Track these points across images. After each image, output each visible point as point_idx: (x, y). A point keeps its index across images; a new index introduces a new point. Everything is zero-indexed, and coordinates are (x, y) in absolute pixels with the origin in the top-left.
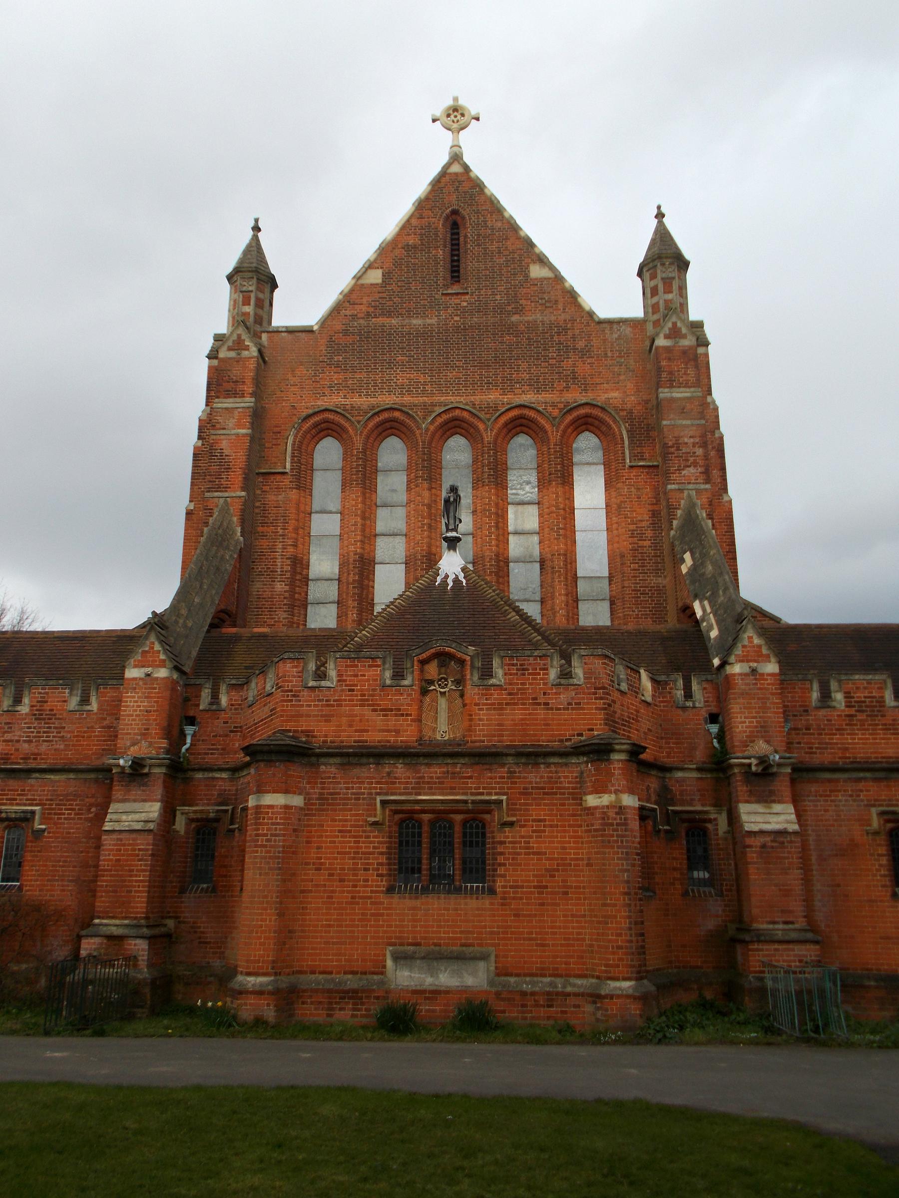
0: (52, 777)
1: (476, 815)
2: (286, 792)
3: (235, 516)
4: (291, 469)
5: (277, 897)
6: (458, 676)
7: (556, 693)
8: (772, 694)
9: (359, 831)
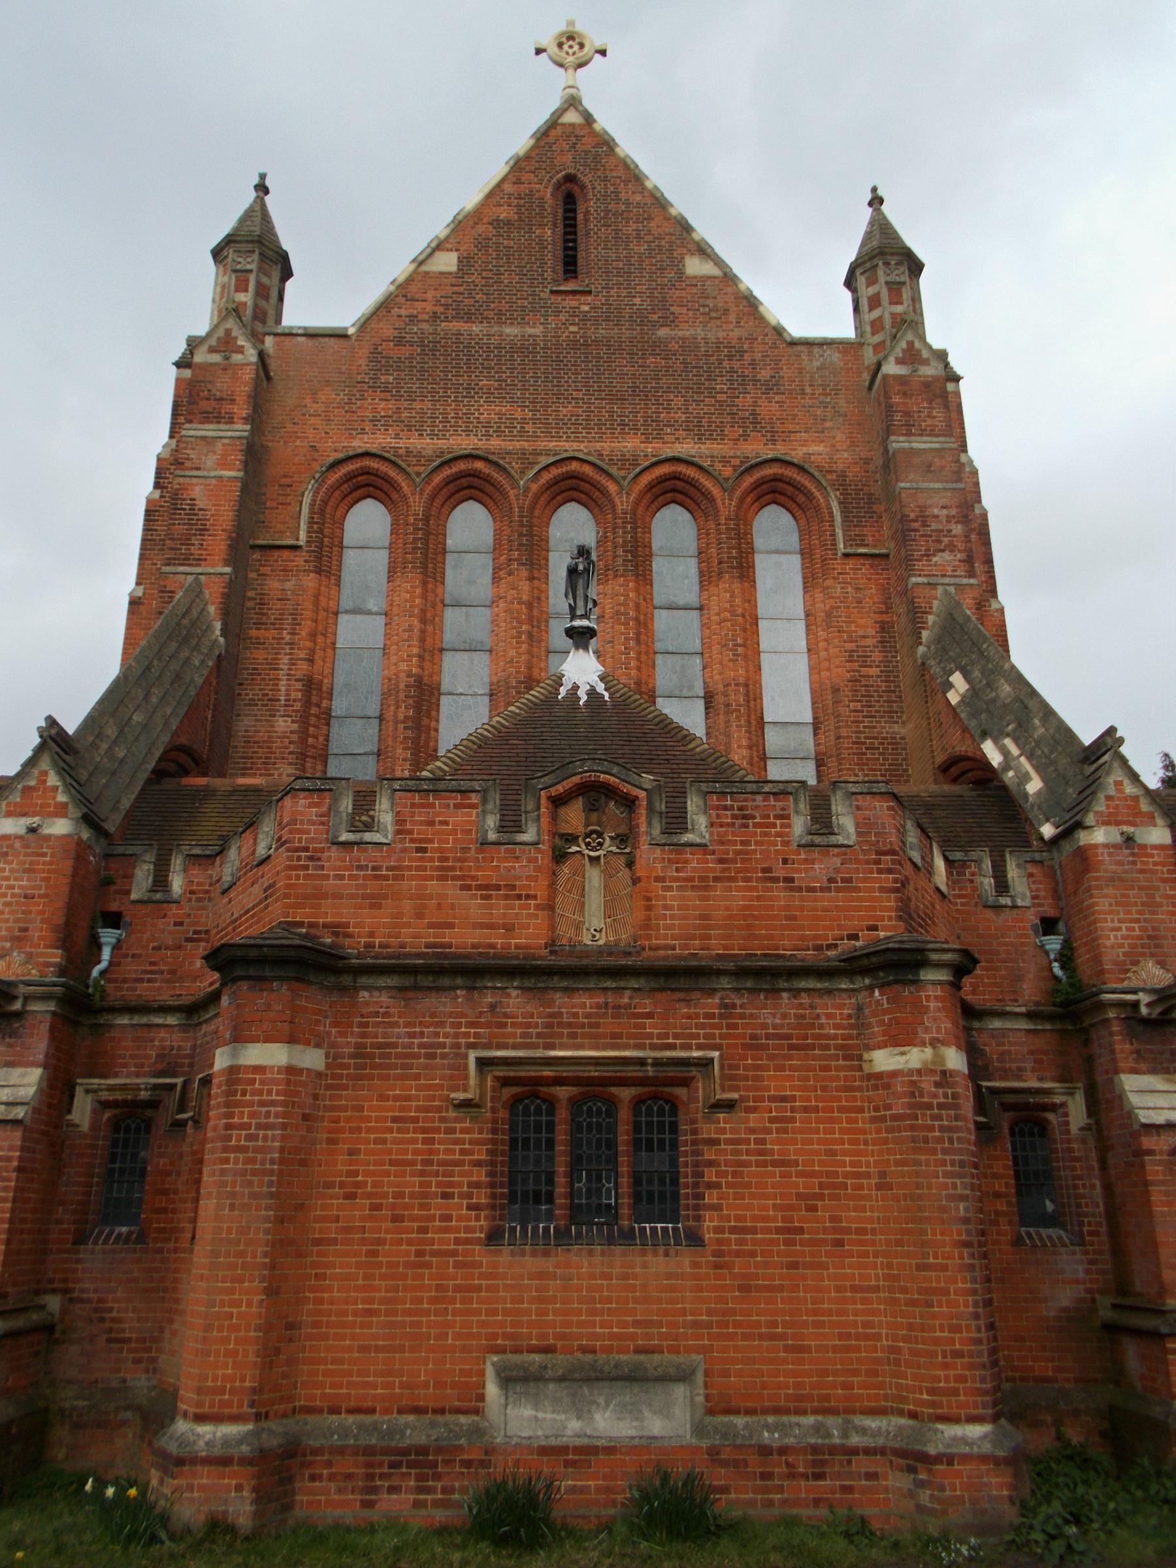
1: (662, 1089)
2: (291, 1040)
3: (212, 603)
4: (308, 542)
5: (266, 1255)
6: (623, 829)
7: (806, 861)
8: (1164, 880)
9: (432, 1120)
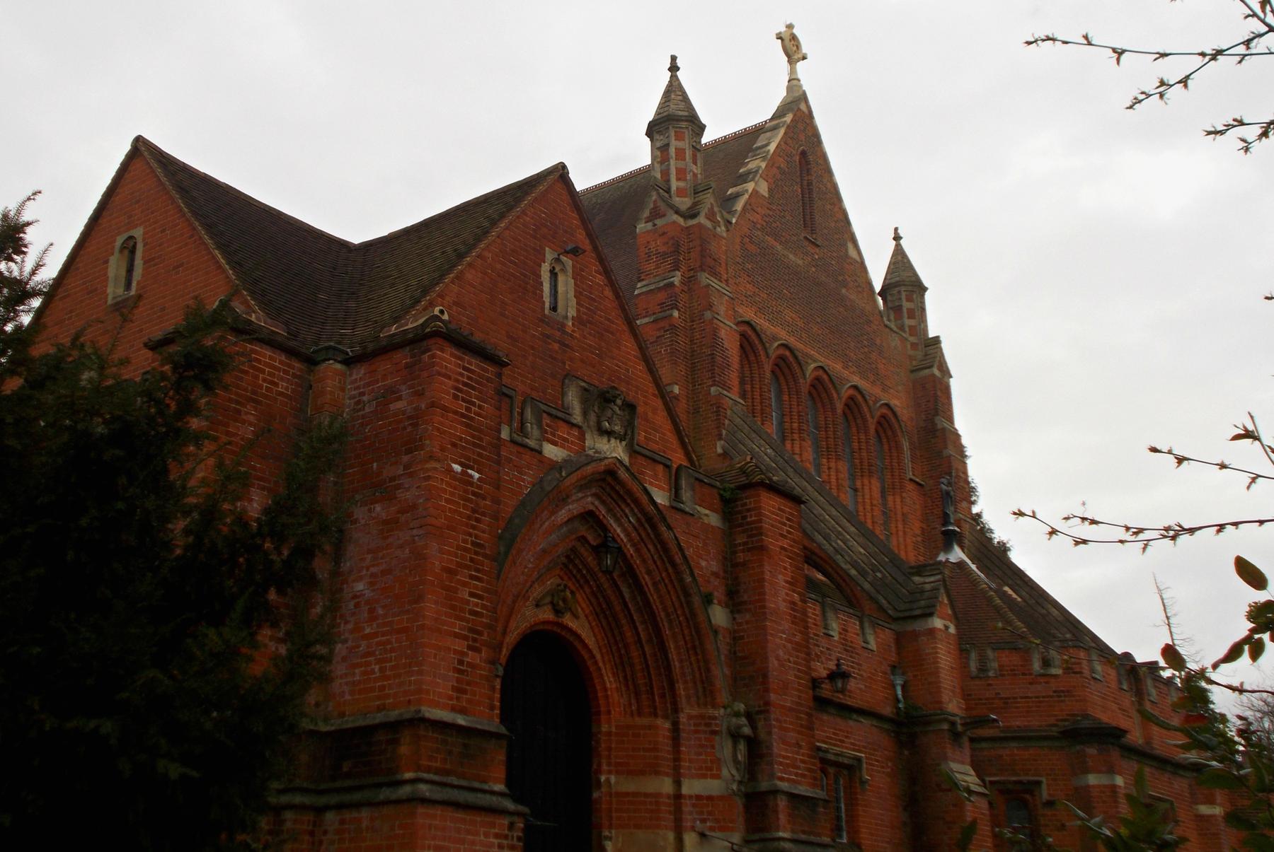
0: (862, 720)
